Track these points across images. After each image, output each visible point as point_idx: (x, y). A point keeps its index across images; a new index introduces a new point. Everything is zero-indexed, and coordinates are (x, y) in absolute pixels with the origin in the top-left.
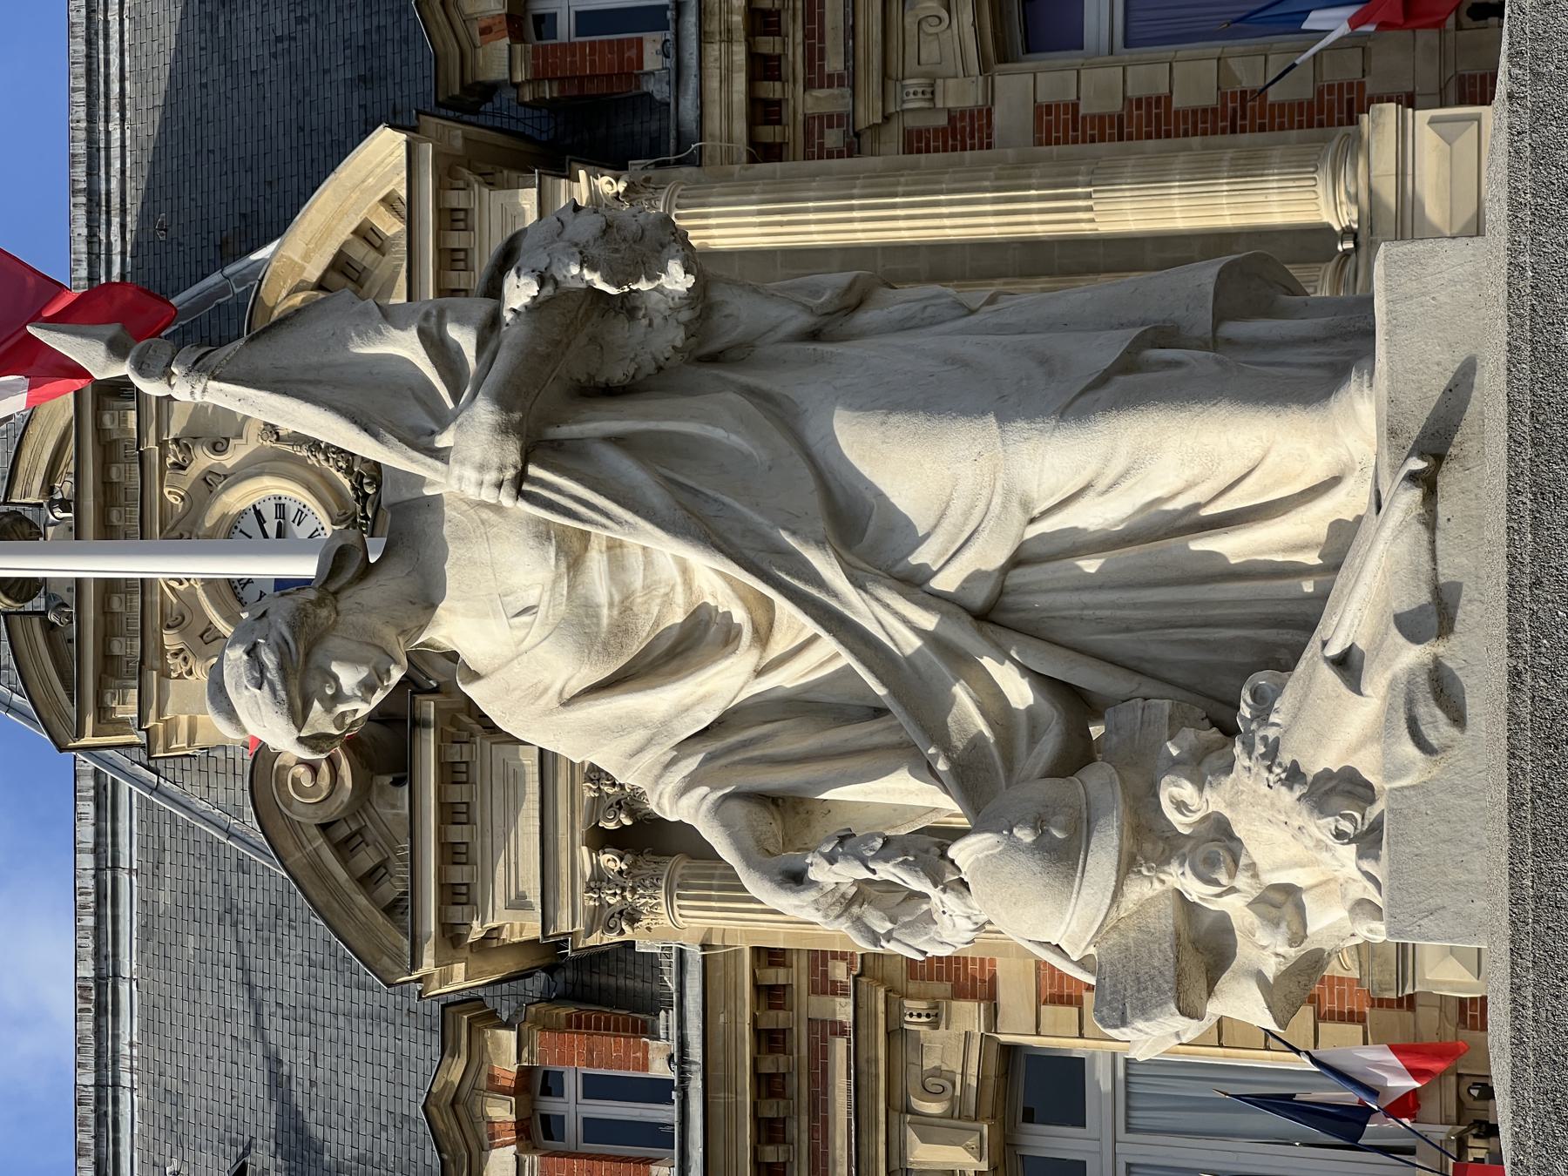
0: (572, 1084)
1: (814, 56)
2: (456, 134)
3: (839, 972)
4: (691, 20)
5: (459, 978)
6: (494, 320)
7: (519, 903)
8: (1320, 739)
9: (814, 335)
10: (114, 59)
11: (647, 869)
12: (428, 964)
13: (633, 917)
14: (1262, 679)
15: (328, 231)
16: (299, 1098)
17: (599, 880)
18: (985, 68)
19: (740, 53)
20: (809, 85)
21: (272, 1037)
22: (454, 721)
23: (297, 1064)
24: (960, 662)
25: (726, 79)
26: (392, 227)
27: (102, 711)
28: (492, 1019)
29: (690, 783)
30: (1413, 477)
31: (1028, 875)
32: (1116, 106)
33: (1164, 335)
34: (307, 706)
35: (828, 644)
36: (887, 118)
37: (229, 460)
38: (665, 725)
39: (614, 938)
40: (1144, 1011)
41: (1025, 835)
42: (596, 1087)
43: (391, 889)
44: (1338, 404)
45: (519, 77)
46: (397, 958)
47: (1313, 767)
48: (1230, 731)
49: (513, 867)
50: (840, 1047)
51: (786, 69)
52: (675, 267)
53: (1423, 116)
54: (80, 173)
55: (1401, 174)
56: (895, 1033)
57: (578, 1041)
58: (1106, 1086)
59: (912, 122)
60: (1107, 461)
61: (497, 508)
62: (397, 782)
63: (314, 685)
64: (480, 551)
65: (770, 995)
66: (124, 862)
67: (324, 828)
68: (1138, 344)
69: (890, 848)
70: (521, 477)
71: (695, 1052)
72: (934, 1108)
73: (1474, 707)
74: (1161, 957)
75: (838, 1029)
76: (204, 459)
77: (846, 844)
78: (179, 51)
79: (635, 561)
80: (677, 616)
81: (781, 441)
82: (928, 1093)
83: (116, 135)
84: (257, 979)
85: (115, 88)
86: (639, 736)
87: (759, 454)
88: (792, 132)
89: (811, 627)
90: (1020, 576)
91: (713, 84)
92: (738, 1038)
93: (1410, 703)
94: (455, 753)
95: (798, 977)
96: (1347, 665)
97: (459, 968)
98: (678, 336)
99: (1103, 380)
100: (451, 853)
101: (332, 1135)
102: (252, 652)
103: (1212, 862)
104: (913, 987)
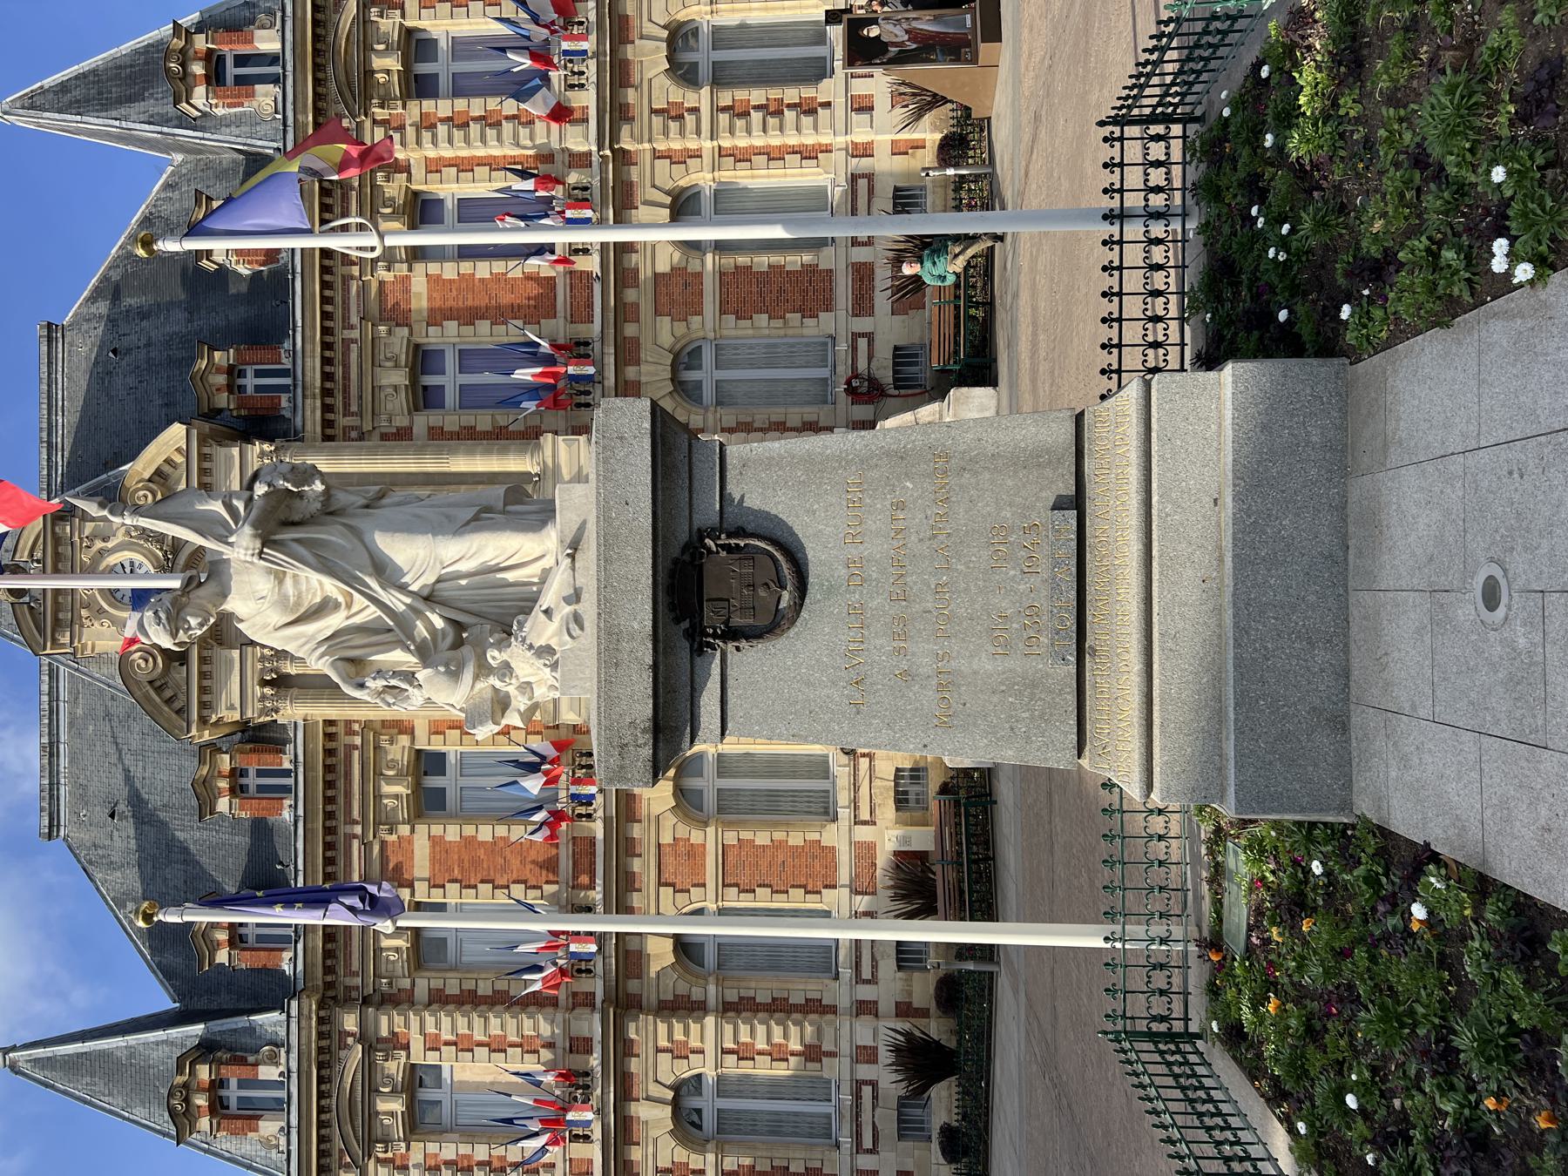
0: (252, 773)
1: (346, 405)
2: (207, 427)
3: (356, 727)
4: (299, 391)
5: (207, 736)
6: (251, 498)
7: (232, 707)
8: (539, 636)
9: (367, 507)
10: (60, 392)
11: (282, 692)
12: (194, 732)
13: (277, 711)
14: (520, 617)
15: (152, 460)
16: (138, 785)
17: (263, 698)
18: (409, 413)
20: (344, 416)
21: (127, 762)
22: (205, 642)
23: (137, 771)
24: (419, 613)
25: (313, 411)
26: (180, 459)
27: (54, 640)
28: (220, 751)
29: (322, 655)
30: (568, 555)
31: (443, 681)
32: (457, 429)
33: (488, 509)
34: (177, 632)
35: (373, 608)
37: (110, 545)
38: (313, 637)
39: (269, 718)
40: (481, 723)
41: (442, 669)
42: (260, 773)
43: (178, 705)
44: (544, 532)
45: (232, 407)
46: (181, 730)
47: (536, 645)
48: (510, 634)
49: (229, 695)
50: (356, 754)
51: (336, 410)
52: (318, 482)
53: (561, 438)
54: (44, 435)
55: (554, 456)
56: (377, 748)
57: (254, 757)
58: (453, 762)
59: (383, 430)
60: (469, 549)
61: (252, 563)
62: (182, 665)
63: (180, 624)
64: (246, 578)
65: (329, 736)
66: (61, 698)
67: (150, 682)
68: (480, 512)
69: (395, 674)
70: (261, 552)
71: (301, 758)
72: (391, 773)
73: (587, 624)
74: (487, 706)
75: (356, 747)
76: (99, 544)
77: (380, 673)
78: (88, 390)
79: (303, 581)
80: (318, 600)
81: (355, 541)
82: (389, 768)
83: (60, 421)
84: (119, 740)
85: (60, 403)
86: (304, 640)
87: (348, 546)
88: (338, 431)
89: (367, 602)
90: (439, 586)
91: (308, 413)
92: (317, 753)
93: (567, 624)
94: (205, 653)
95: (340, 729)
96: (547, 612)
97: (207, 732)
98: (319, 506)
99: (468, 523)
100: (203, 690)
101: (152, 797)
102: (156, 613)
103: (504, 675)
104: (384, 731)
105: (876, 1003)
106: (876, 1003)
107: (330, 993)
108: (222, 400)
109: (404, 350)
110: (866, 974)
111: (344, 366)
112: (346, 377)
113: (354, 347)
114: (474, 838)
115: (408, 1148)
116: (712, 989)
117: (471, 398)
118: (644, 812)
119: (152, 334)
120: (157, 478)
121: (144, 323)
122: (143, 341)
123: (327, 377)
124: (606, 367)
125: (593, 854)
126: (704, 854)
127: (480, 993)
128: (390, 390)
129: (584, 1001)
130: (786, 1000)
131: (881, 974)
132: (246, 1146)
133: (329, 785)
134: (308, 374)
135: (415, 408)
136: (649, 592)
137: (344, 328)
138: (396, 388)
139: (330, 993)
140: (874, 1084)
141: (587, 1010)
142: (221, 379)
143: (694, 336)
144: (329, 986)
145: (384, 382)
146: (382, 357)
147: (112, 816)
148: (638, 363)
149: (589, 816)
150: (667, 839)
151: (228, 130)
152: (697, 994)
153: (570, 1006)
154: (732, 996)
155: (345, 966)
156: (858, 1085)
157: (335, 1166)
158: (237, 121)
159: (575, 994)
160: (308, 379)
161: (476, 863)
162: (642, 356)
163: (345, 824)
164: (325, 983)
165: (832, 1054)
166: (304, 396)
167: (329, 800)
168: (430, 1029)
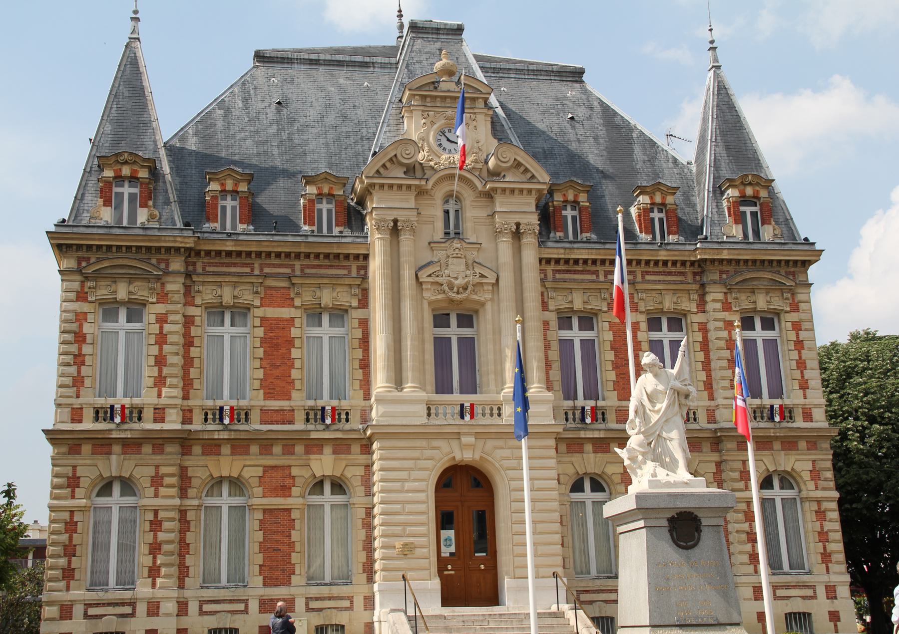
1: (559, 271)
18: (556, 310)
19: (562, 256)
20: (553, 270)
25: (558, 254)
36: (547, 288)
43: (382, 171)
51: (556, 265)
62: (405, 173)
65: (357, 257)
67: (396, 155)
104: (360, 290)
105: (186, 615)
106: (186, 615)
107: (193, 254)
108: (558, 197)
109: (594, 307)
110: (206, 608)
111: (582, 271)
112: (575, 272)
113: (594, 277)
114: (293, 346)
115: (91, 302)
116: (195, 502)
117: (566, 346)
118: (312, 457)
119: (586, 145)
120: (516, 163)
121: (592, 140)
122: (581, 138)
123: (576, 261)
124: (591, 432)
125: (283, 423)
126: (284, 496)
127: (192, 349)
128: (570, 299)
129: (187, 419)
130: (188, 553)
131: (206, 617)
132: (93, 200)
133: (327, 256)
134: (578, 251)
135: (558, 311)
136: (687, 506)
137: (605, 271)
138: (572, 302)
139: (193, 254)
140: (133, 615)
141: (181, 420)
142: (571, 197)
143: (612, 487)
144: (198, 253)
145: (575, 295)
146: (589, 294)
147: (279, 103)
148: (594, 452)
149: (308, 420)
150: (295, 471)
151: (714, 207)
152: (191, 492)
153: (183, 408)
154: (190, 516)
155: (208, 263)
156: (133, 604)
157: (80, 254)
158: (720, 212)
159: (191, 411)
160: (576, 251)
161: (277, 347)
162: (599, 455)
163: (301, 265)
164: (200, 251)
165: (154, 585)
166: (565, 249)
167: (317, 256)
168: (171, 318)
